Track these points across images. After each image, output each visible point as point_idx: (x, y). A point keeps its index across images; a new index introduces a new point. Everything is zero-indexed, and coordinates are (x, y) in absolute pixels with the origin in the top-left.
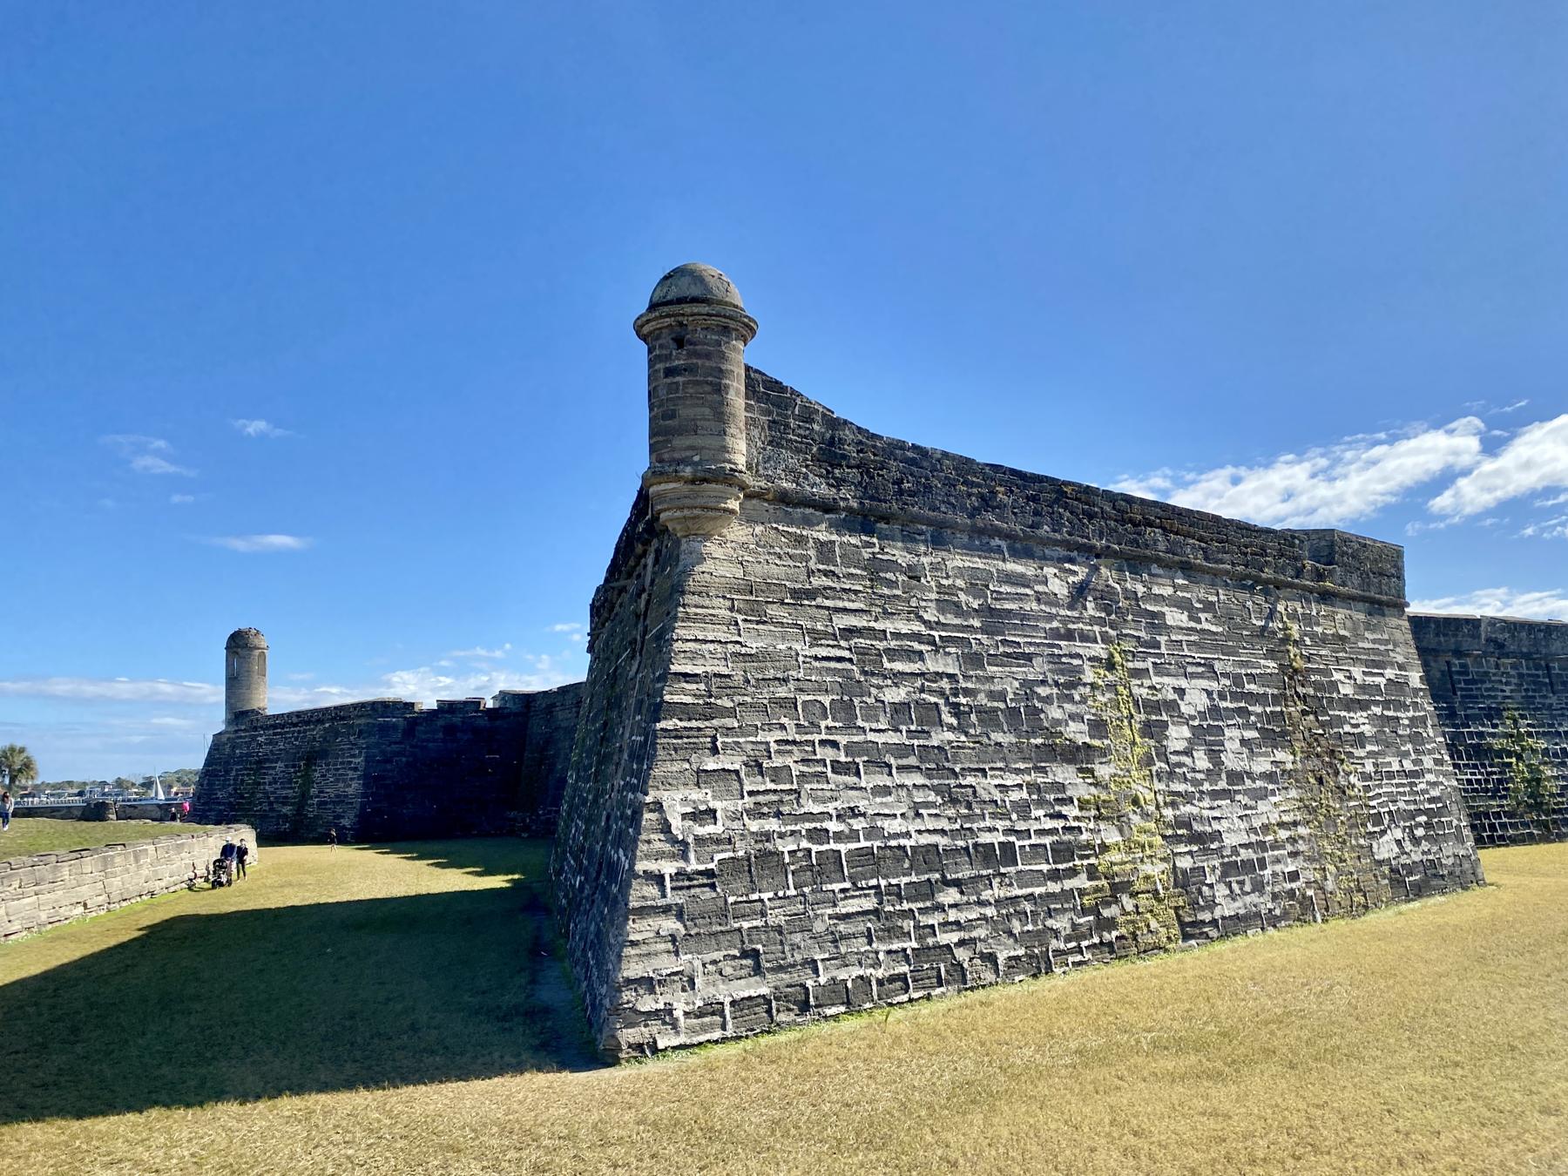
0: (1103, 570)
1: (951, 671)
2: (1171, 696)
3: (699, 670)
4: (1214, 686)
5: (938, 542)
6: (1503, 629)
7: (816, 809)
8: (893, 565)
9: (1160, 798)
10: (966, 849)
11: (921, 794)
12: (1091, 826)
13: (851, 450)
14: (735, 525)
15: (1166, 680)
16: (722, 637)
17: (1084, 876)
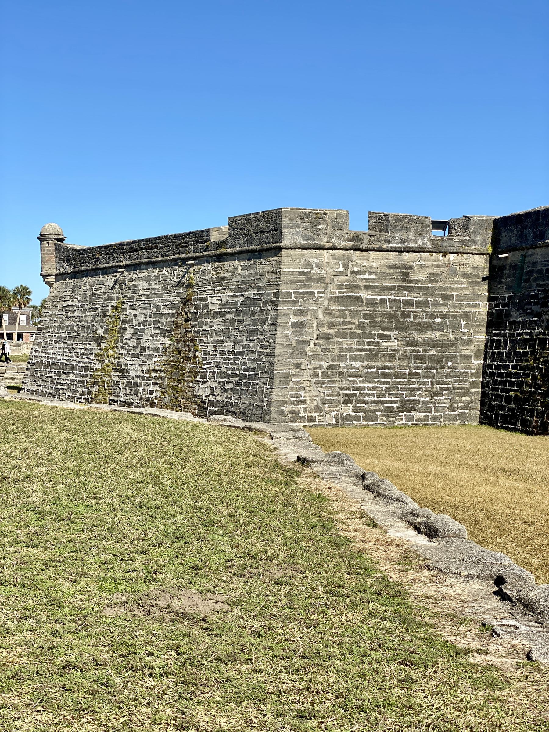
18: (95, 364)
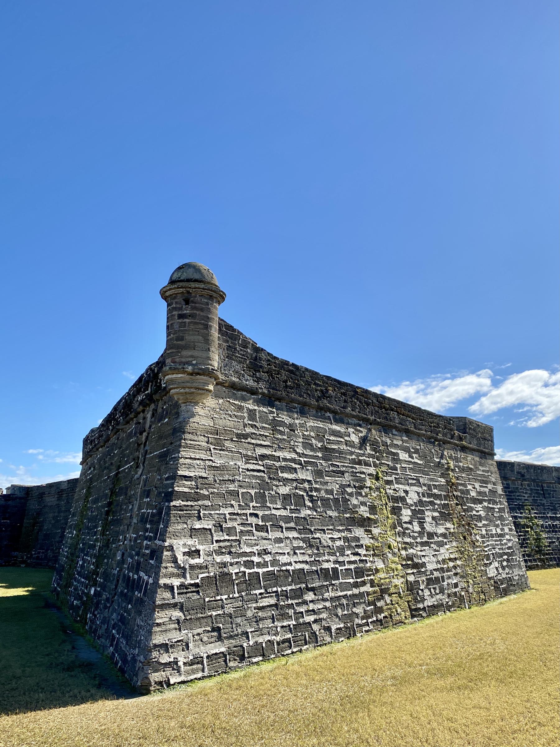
0: (373, 431)
1: (309, 479)
2: (403, 494)
3: (192, 474)
4: (420, 490)
5: (302, 413)
6: (523, 468)
7: (248, 550)
8: (282, 424)
9: (400, 545)
10: (317, 571)
11: (296, 542)
12: (371, 559)
13: (264, 363)
14: (209, 398)
15: (400, 486)
16: (203, 457)
17: (369, 585)
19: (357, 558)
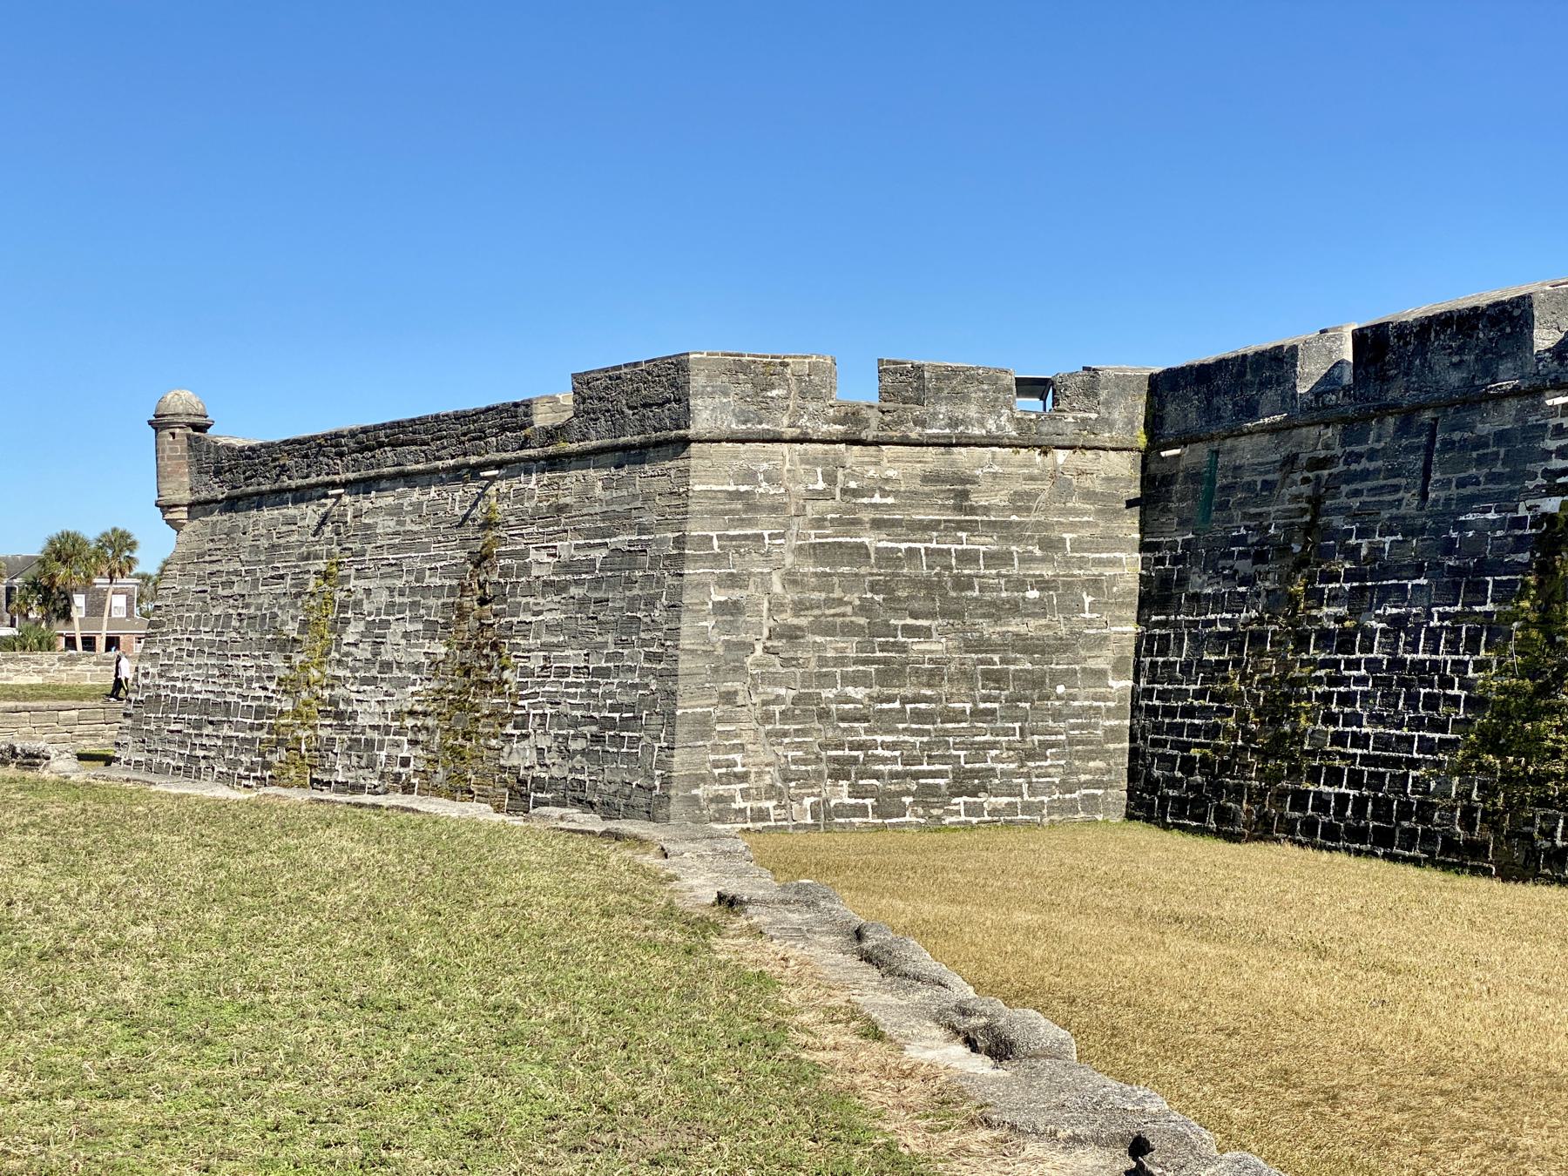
18: (279, 701)
19: (262, 693)
